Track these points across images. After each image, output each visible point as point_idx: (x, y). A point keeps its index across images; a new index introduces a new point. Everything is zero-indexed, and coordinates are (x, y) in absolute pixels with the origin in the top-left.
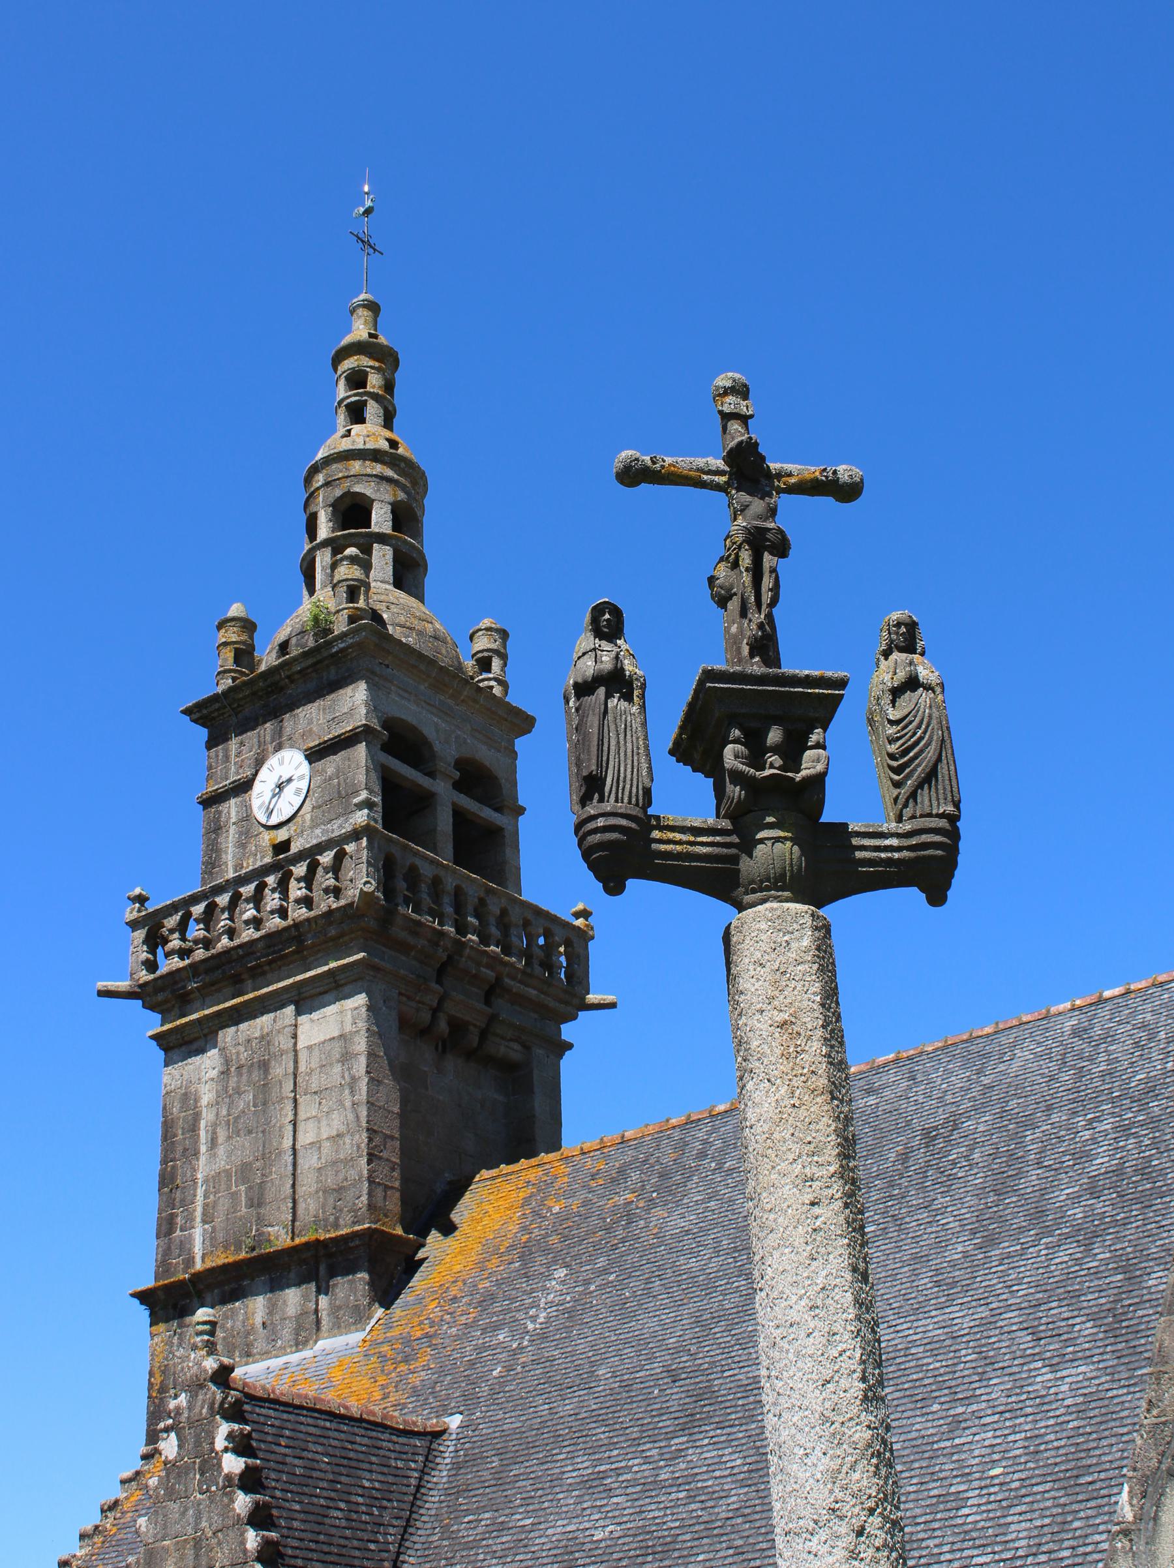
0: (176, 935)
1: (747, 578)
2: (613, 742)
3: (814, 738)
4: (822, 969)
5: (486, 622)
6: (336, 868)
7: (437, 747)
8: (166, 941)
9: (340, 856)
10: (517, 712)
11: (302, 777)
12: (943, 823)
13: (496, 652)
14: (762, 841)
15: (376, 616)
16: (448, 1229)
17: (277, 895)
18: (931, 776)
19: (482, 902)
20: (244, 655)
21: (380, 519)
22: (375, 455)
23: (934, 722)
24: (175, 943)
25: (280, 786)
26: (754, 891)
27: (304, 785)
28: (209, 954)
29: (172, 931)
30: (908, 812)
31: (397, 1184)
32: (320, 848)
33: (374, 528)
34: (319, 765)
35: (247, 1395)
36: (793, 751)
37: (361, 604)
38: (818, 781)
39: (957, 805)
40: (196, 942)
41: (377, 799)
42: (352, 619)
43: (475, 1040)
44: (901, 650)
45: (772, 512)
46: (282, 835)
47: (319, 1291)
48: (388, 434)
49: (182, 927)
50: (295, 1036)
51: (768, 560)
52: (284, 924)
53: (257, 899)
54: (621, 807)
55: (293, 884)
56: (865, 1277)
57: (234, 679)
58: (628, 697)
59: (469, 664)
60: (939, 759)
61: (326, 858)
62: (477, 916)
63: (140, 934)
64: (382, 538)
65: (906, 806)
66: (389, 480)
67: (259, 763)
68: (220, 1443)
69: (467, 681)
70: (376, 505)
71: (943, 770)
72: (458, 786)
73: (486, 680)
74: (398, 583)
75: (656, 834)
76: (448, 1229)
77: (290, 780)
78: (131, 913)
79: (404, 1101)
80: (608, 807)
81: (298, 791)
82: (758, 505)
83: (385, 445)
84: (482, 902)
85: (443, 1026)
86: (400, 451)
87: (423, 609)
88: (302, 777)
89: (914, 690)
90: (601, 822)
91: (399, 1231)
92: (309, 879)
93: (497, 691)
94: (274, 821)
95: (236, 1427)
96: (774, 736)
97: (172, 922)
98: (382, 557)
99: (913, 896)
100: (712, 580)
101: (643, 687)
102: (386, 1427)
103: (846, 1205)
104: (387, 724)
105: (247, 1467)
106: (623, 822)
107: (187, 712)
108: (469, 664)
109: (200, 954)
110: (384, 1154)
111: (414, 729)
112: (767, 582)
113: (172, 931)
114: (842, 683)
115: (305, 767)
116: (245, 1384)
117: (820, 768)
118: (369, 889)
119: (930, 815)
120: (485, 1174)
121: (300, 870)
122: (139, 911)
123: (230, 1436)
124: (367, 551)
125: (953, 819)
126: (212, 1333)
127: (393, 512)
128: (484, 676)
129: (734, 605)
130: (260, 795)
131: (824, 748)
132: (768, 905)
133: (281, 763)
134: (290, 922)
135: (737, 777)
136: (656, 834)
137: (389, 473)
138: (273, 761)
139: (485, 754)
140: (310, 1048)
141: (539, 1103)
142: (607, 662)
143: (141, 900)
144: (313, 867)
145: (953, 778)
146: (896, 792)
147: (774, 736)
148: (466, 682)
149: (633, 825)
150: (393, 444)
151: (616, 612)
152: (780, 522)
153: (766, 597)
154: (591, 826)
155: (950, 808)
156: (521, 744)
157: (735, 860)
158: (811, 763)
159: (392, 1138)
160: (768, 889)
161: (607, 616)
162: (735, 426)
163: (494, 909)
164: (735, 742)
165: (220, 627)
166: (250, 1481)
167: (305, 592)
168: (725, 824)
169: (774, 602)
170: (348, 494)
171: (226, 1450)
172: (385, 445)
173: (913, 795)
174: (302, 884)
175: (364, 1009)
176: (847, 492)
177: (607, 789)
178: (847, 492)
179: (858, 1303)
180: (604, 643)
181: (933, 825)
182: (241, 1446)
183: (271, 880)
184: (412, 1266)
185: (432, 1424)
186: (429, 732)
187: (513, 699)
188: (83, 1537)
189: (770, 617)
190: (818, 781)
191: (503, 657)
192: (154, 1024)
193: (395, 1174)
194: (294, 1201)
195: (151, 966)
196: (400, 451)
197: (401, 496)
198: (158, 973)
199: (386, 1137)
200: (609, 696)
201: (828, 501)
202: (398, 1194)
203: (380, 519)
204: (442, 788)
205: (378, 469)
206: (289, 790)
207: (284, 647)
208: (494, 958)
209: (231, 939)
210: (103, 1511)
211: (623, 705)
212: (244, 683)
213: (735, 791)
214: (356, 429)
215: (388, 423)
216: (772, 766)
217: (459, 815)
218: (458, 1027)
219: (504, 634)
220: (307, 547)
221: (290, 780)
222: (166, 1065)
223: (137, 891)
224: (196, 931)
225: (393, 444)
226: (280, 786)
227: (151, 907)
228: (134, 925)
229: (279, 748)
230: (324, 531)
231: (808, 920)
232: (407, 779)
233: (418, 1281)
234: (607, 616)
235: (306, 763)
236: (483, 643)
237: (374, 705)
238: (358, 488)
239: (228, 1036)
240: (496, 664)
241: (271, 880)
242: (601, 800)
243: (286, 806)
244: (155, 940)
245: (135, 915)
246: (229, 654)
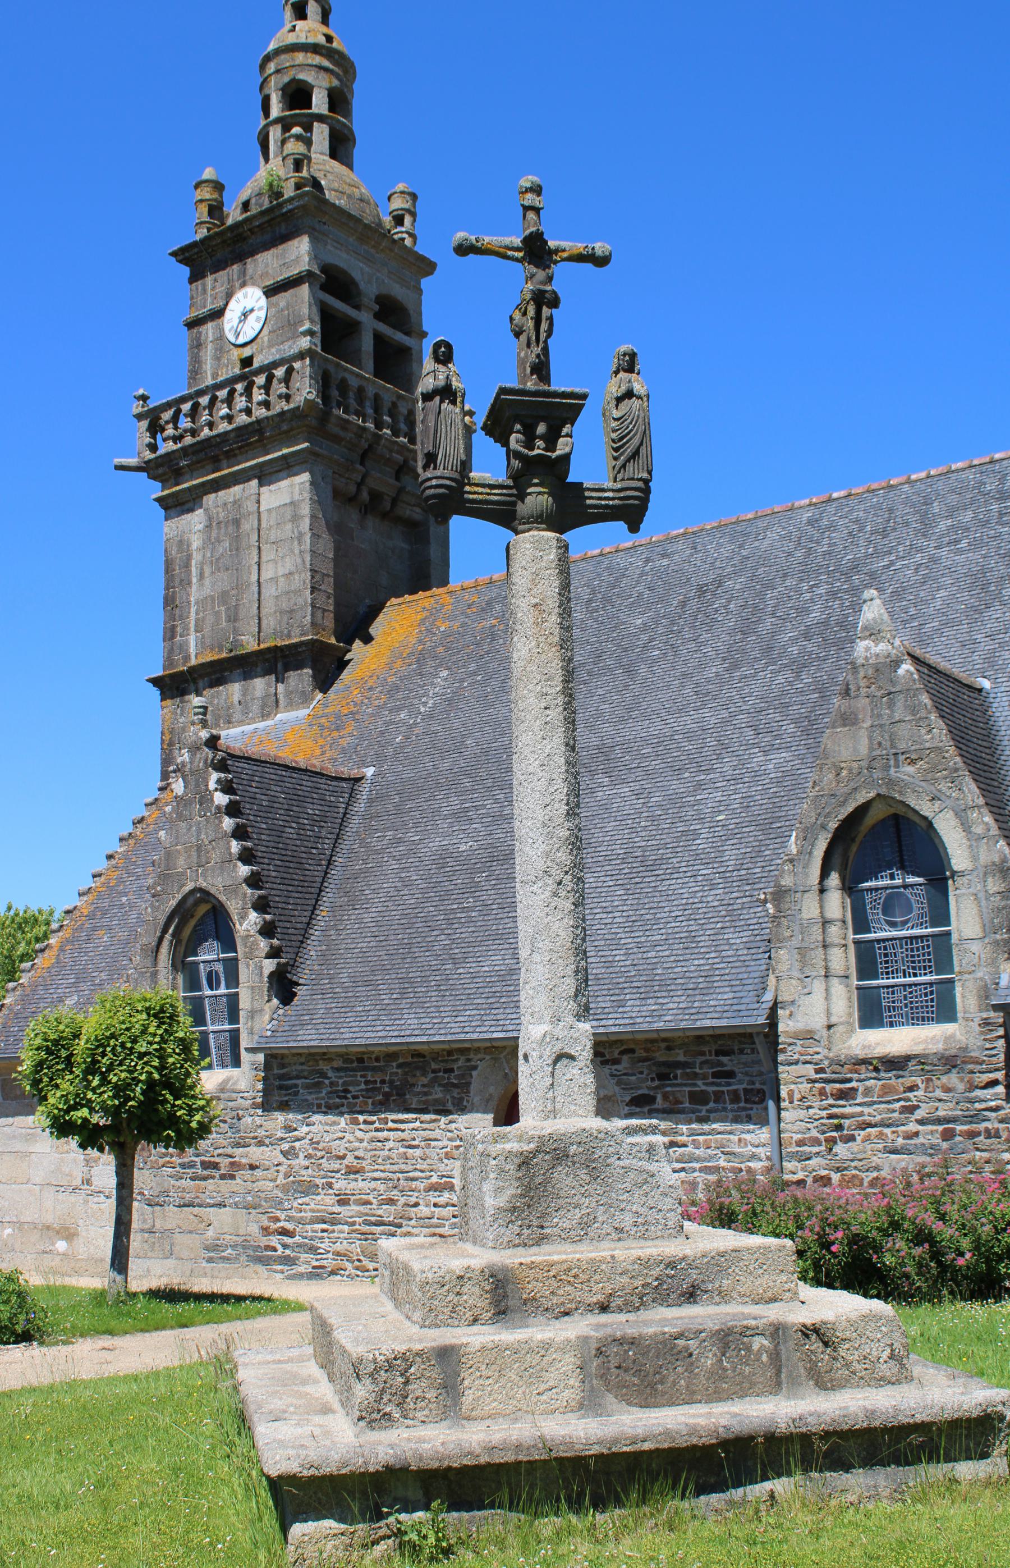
0: (171, 425)
1: (531, 324)
2: (443, 430)
3: (565, 430)
4: (561, 572)
5: (401, 187)
6: (287, 380)
7: (362, 286)
8: (163, 430)
9: (290, 371)
10: (423, 259)
11: (261, 309)
12: (640, 484)
13: (408, 211)
14: (530, 494)
15: (316, 184)
16: (368, 639)
17: (244, 399)
18: (636, 453)
19: (394, 405)
20: (216, 210)
21: (319, 103)
22: (314, 49)
23: (640, 420)
24: (170, 431)
25: (245, 315)
26: (524, 523)
27: (262, 314)
28: (195, 440)
29: (167, 423)
30: (620, 476)
31: (331, 608)
32: (275, 365)
33: (315, 110)
34: (274, 299)
35: (229, 754)
36: (551, 439)
37: (305, 173)
38: (566, 458)
39: (650, 473)
40: (186, 431)
41: (317, 328)
42: (298, 186)
43: (387, 505)
44: (625, 371)
45: (550, 279)
46: (247, 352)
47: (277, 681)
48: (324, 29)
49: (175, 419)
50: (258, 502)
51: (546, 311)
52: (249, 420)
53: (229, 401)
54: (447, 473)
55: (255, 390)
56: (573, 749)
57: (209, 230)
58: (454, 402)
59: (387, 220)
60: (641, 444)
61: (280, 372)
62: (390, 416)
63: (144, 424)
64: (320, 118)
65: (619, 472)
66: (326, 70)
67: (229, 296)
68: (212, 785)
69: (386, 235)
70: (316, 91)
71: (643, 450)
72: (378, 316)
73: (399, 233)
74: (333, 155)
75: (467, 488)
76: (368, 639)
77: (252, 310)
78: (137, 408)
79: (337, 549)
80: (438, 473)
81: (258, 319)
82: (541, 275)
83: (322, 40)
84: (394, 405)
85: (365, 496)
86: (335, 45)
87: (353, 176)
88: (261, 309)
89: (630, 398)
90: (434, 482)
91: (333, 641)
92: (267, 387)
93: (408, 242)
94: (241, 340)
95: (222, 775)
96: (541, 429)
97: (167, 415)
98: (321, 133)
99: (621, 526)
100: (511, 319)
101: (463, 396)
102: (323, 775)
103: (565, 709)
104: (325, 269)
105: (230, 801)
106: (448, 482)
107: (174, 254)
108: (387, 220)
109: (188, 440)
110: (323, 587)
111: (344, 272)
112: (544, 326)
113: (167, 423)
114: (584, 397)
115: (263, 301)
116: (228, 747)
117: (567, 450)
118: (311, 397)
119: (633, 479)
120: (394, 601)
121: (261, 380)
122: (143, 407)
123: (218, 781)
124: (308, 128)
125: (647, 482)
126: (205, 714)
127: (330, 96)
128: (399, 229)
129: (523, 338)
130: (229, 322)
131: (571, 437)
132: (531, 533)
133: (246, 296)
134: (254, 419)
135: (517, 455)
136: (467, 488)
137: (326, 63)
138: (239, 295)
139: (398, 291)
140: (269, 511)
141: (434, 551)
142: (441, 382)
143: (144, 398)
144: (270, 379)
145: (650, 455)
146: (614, 463)
147: (541, 429)
148: (385, 235)
149: (454, 484)
150: (329, 39)
151: (449, 346)
152: (555, 286)
153: (543, 336)
154: (428, 484)
155: (645, 475)
156: (425, 283)
157: (514, 504)
158: (562, 447)
159: (328, 575)
160: (532, 523)
161: (443, 349)
162: (531, 215)
163: (403, 410)
164: (518, 432)
165: (197, 186)
166: (233, 809)
167: (262, 160)
168: (510, 482)
169: (550, 332)
170: (294, 81)
171: (216, 790)
172: (322, 40)
173: (624, 466)
174: (263, 391)
175: (308, 484)
176: (601, 261)
177: (439, 461)
178: (601, 261)
179: (568, 763)
180: (440, 366)
181: (634, 485)
182: (227, 788)
183: (239, 387)
184: (342, 665)
185: (355, 773)
186: (356, 275)
187: (420, 249)
188: (121, 840)
189: (546, 350)
190: (566, 458)
191: (413, 214)
192: (156, 490)
193: (331, 601)
194: (259, 619)
195: (153, 448)
196: (335, 45)
197: (336, 83)
198: (159, 453)
199: (324, 575)
200: (442, 401)
201: (589, 266)
202: (332, 615)
203: (319, 103)
204: (365, 318)
205: (318, 60)
206: (252, 318)
207: (246, 206)
208: (403, 446)
209: (211, 430)
210: (134, 823)
211: (451, 407)
212: (217, 234)
213: (516, 463)
214: (300, 24)
215: (325, 20)
216: (538, 448)
217: (378, 337)
218: (376, 496)
219: (414, 197)
220: (263, 123)
221: (252, 310)
222: (166, 519)
223: (141, 392)
224: (185, 423)
225: (329, 39)
226: (245, 315)
227: (152, 404)
228: (139, 417)
229: (243, 285)
230: (276, 110)
231: (554, 543)
232: (338, 310)
233: (345, 675)
234: (443, 349)
235: (264, 298)
236: (398, 203)
237: (315, 255)
238: (301, 76)
239: (210, 500)
240: (408, 220)
241: (239, 387)
242: (435, 468)
243: (251, 328)
244: (155, 428)
245: (140, 410)
246: (204, 209)
